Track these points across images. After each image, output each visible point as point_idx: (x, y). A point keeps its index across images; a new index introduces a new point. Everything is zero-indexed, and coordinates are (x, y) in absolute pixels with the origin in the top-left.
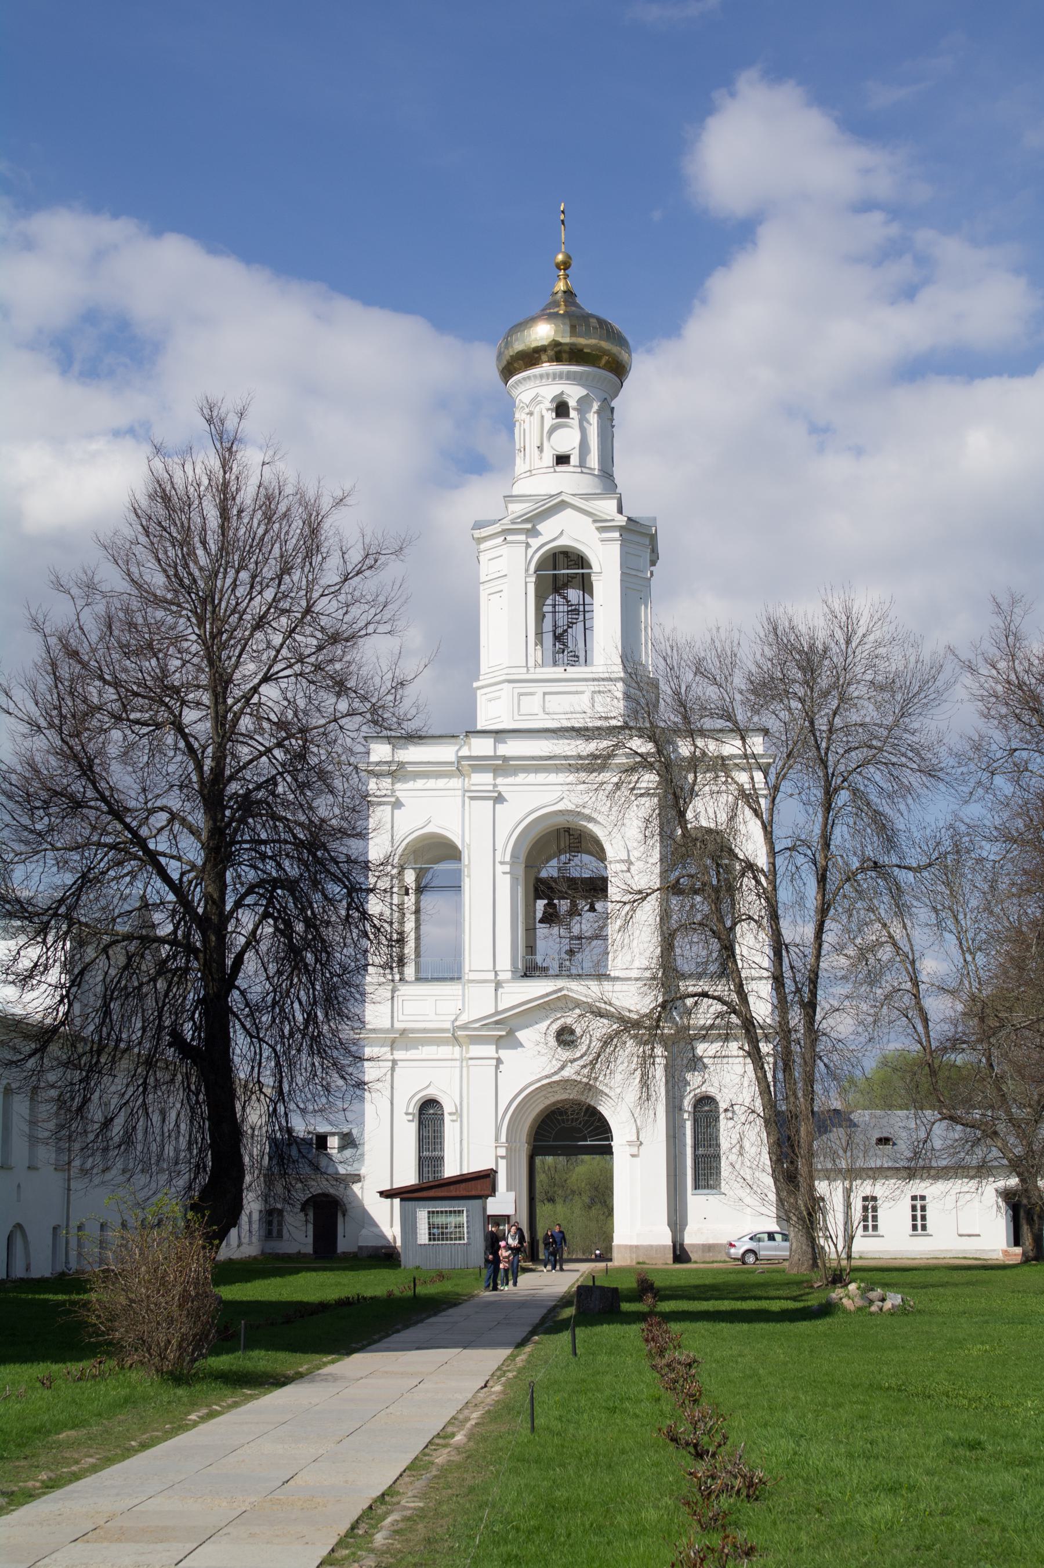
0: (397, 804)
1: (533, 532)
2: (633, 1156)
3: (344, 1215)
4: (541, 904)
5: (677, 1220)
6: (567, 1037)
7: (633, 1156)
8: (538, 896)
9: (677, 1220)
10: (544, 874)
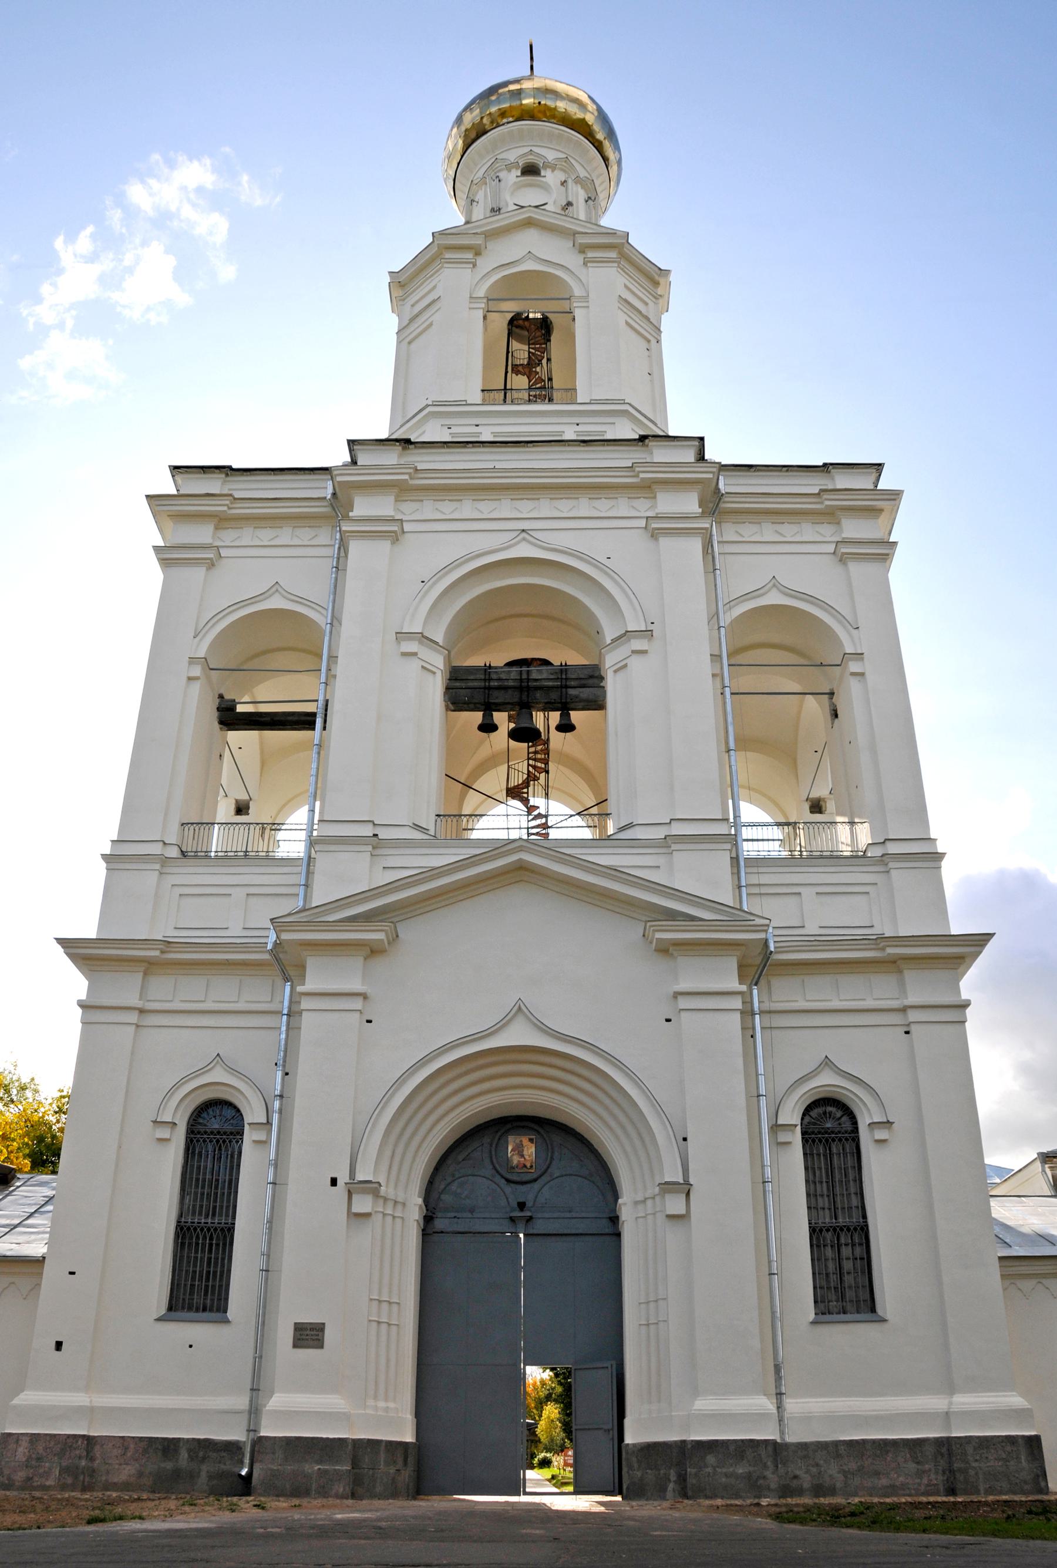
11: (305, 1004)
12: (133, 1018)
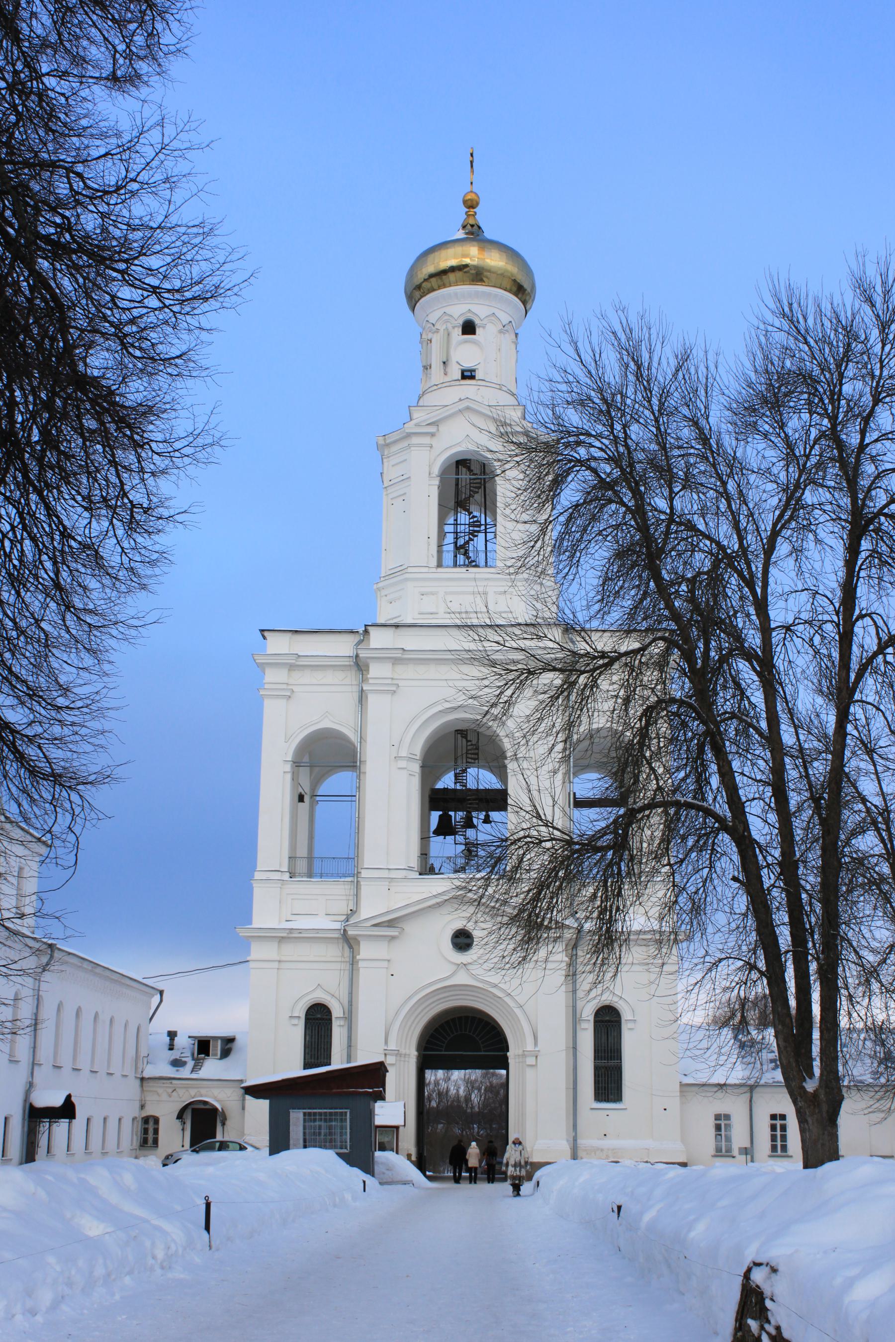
3: (223, 1124)
4: (435, 816)
8: (433, 808)
10: (440, 785)
11: (361, 964)
12: (276, 965)
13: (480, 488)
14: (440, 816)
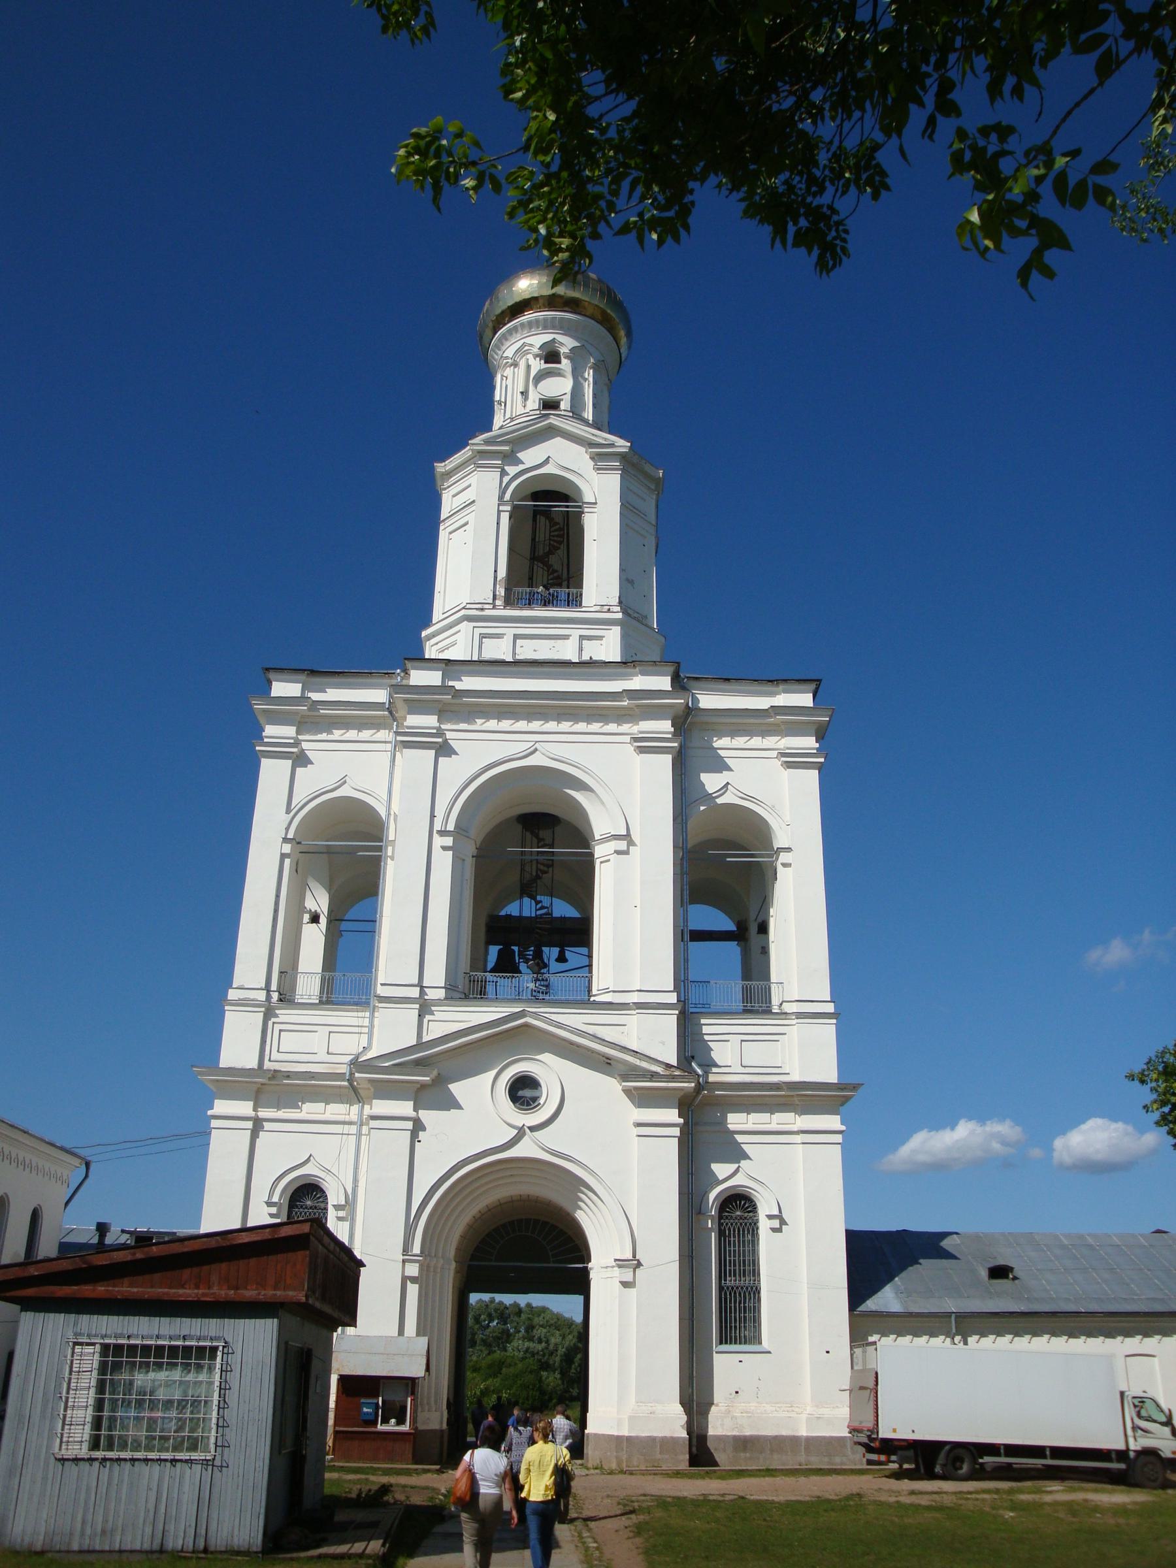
0: (301, 760)
1: (510, 458)
2: (625, 1284)
4: (494, 951)
5: (696, 1395)
6: (527, 1093)
7: (625, 1284)
8: (489, 942)
9: (696, 1395)
13: (560, 543)
14: (500, 951)
